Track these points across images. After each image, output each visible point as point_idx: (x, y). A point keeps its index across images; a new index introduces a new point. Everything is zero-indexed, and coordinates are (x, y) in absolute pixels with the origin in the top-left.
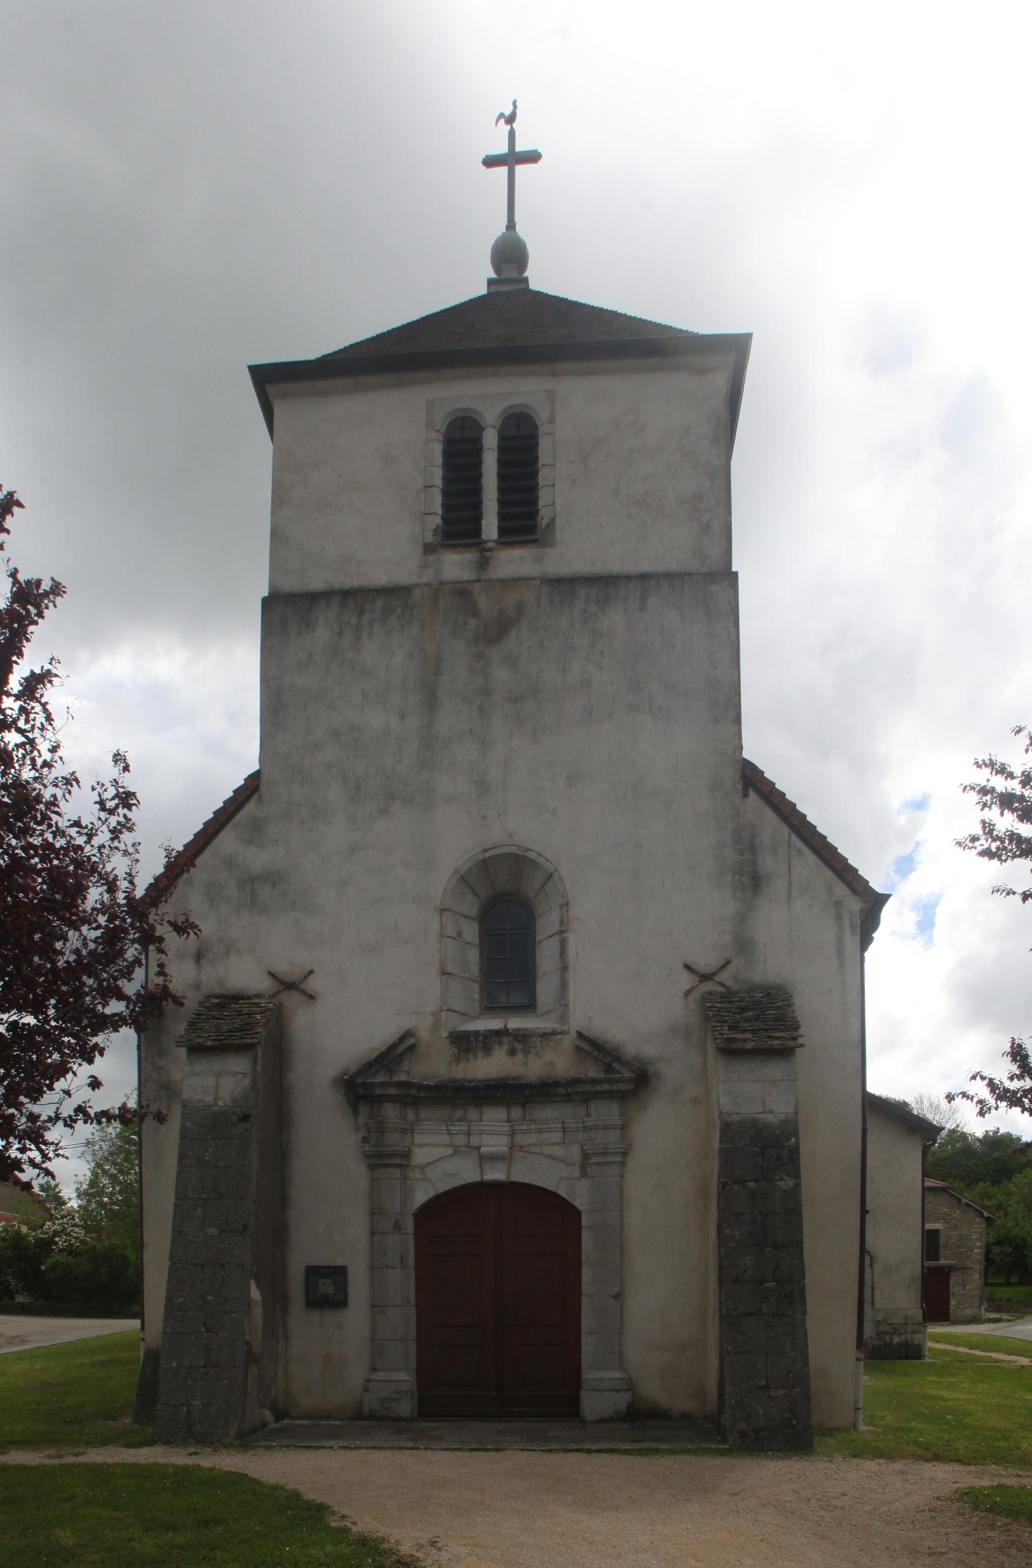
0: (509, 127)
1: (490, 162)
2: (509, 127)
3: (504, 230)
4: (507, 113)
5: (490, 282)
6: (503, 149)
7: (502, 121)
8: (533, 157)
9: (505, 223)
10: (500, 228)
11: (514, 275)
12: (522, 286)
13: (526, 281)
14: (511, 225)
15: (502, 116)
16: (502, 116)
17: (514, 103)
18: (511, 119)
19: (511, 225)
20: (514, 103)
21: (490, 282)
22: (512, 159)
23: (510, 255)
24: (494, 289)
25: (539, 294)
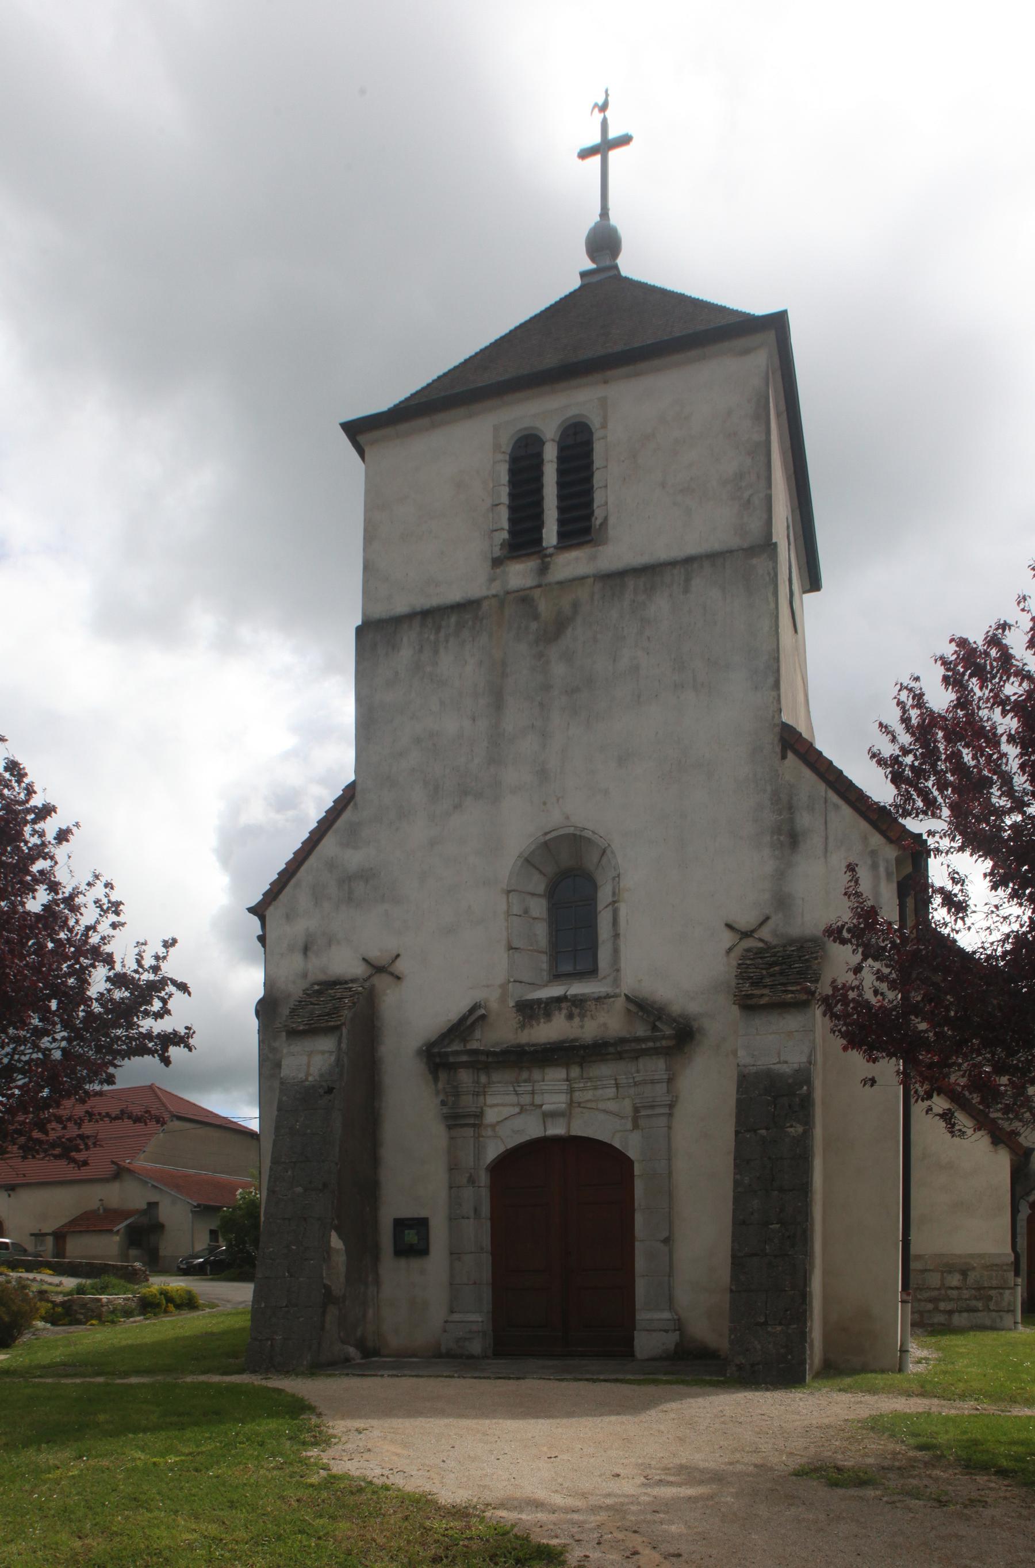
0: (602, 115)
1: (585, 154)
2: (602, 115)
3: (598, 219)
4: (600, 102)
5: (583, 275)
6: (596, 139)
7: (596, 110)
8: (625, 140)
9: (598, 210)
10: (593, 217)
11: (608, 263)
12: (614, 272)
13: (616, 267)
14: (604, 213)
15: (596, 105)
16: (596, 105)
17: (606, 92)
18: (604, 108)
19: (604, 213)
20: (606, 92)
21: (583, 275)
22: (604, 147)
23: (604, 243)
24: (588, 280)
25: (626, 279)
